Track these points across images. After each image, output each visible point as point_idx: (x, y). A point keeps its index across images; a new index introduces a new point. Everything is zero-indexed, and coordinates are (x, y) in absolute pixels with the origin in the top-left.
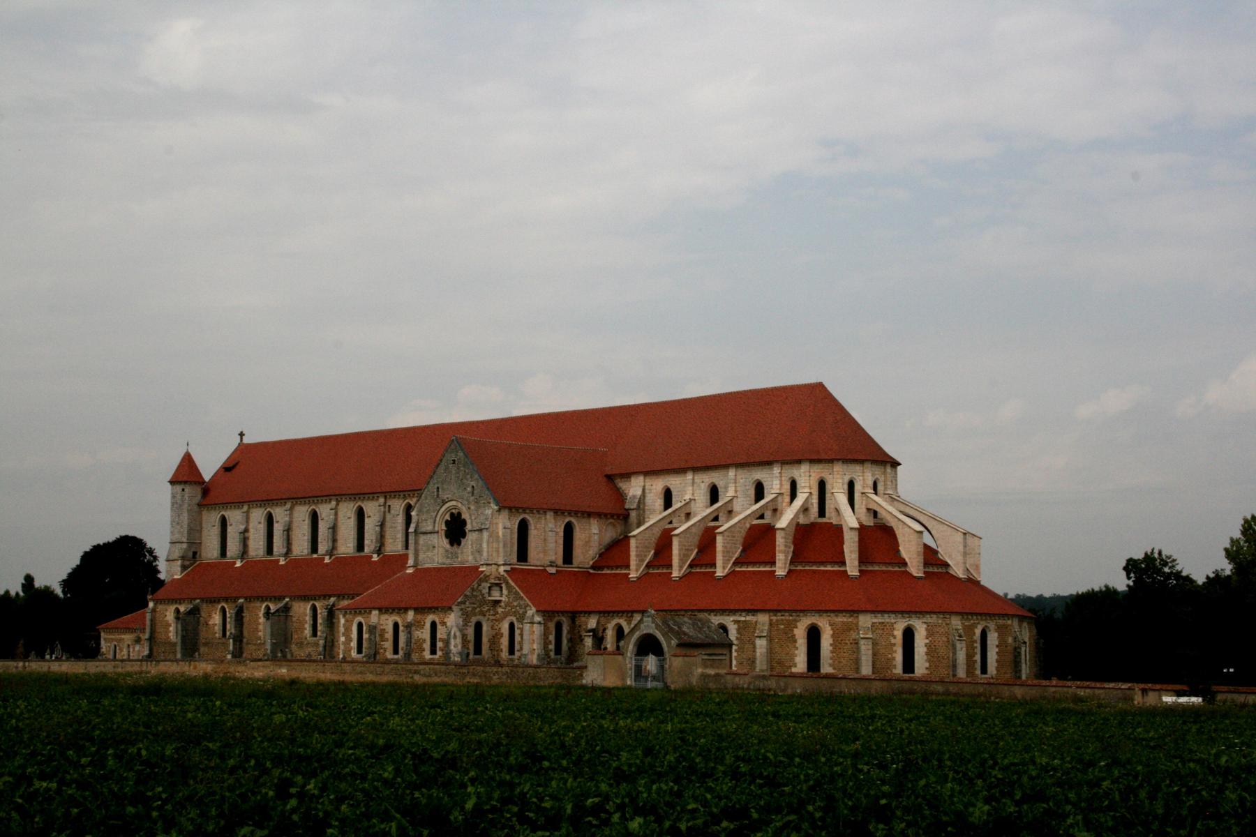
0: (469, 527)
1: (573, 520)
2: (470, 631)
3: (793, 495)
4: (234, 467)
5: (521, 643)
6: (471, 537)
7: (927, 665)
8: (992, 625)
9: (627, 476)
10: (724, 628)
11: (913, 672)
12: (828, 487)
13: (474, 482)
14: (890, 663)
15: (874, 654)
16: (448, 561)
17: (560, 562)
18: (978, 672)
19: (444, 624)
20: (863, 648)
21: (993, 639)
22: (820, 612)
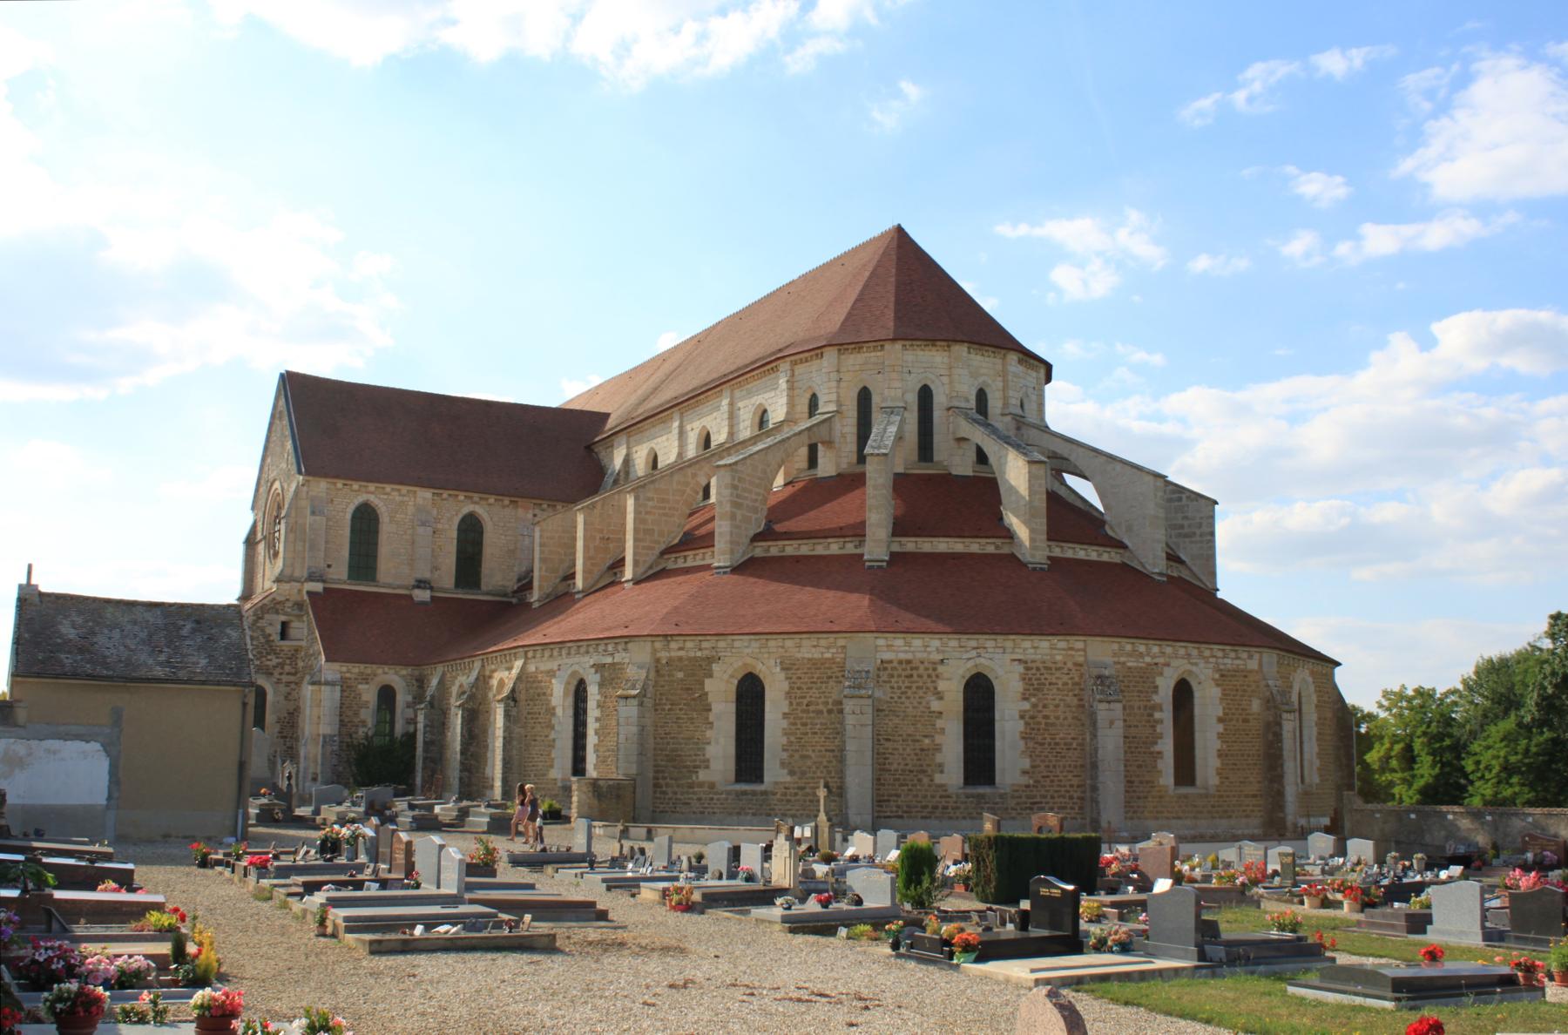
1: (480, 510)
7: (1026, 763)
11: (990, 779)
14: (925, 759)
15: (877, 739)
17: (446, 577)
18: (1167, 777)
20: (850, 720)
21: (1208, 703)
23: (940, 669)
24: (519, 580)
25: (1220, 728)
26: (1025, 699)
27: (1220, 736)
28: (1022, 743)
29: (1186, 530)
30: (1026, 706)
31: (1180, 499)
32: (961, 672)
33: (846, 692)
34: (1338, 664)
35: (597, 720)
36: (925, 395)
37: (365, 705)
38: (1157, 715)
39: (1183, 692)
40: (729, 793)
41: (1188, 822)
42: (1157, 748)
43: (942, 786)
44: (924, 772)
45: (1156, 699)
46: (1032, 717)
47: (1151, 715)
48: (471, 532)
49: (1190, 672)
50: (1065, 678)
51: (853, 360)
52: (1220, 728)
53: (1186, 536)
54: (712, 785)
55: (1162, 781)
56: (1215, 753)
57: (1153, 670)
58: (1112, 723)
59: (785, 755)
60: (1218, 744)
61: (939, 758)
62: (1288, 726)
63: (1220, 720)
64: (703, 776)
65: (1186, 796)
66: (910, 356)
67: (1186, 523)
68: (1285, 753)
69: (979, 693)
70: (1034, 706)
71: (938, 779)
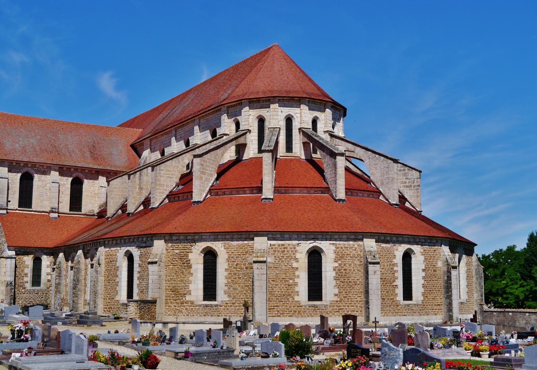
7: (336, 291)
8: (417, 249)
11: (320, 299)
12: (267, 125)
17: (65, 207)
20: (256, 272)
21: (418, 263)
22: (217, 236)
23: (297, 248)
24: (100, 207)
25: (424, 274)
26: (336, 261)
27: (424, 278)
28: (335, 281)
29: (407, 184)
30: (336, 265)
31: (404, 170)
32: (307, 249)
33: (254, 259)
34: (476, 245)
35: (139, 272)
37: (27, 267)
38: (395, 269)
40: (200, 306)
41: (409, 317)
42: (395, 284)
43: (298, 301)
44: (290, 295)
45: (395, 261)
46: (339, 270)
47: (392, 269)
49: (410, 249)
50: (354, 252)
52: (424, 274)
53: (407, 187)
54: (192, 303)
55: (398, 299)
56: (421, 286)
58: (375, 272)
59: (226, 288)
60: (423, 282)
61: (297, 289)
62: (454, 273)
63: (424, 270)
64: (188, 298)
65: (408, 305)
67: (407, 181)
68: (453, 285)
70: (340, 265)
71: (296, 298)
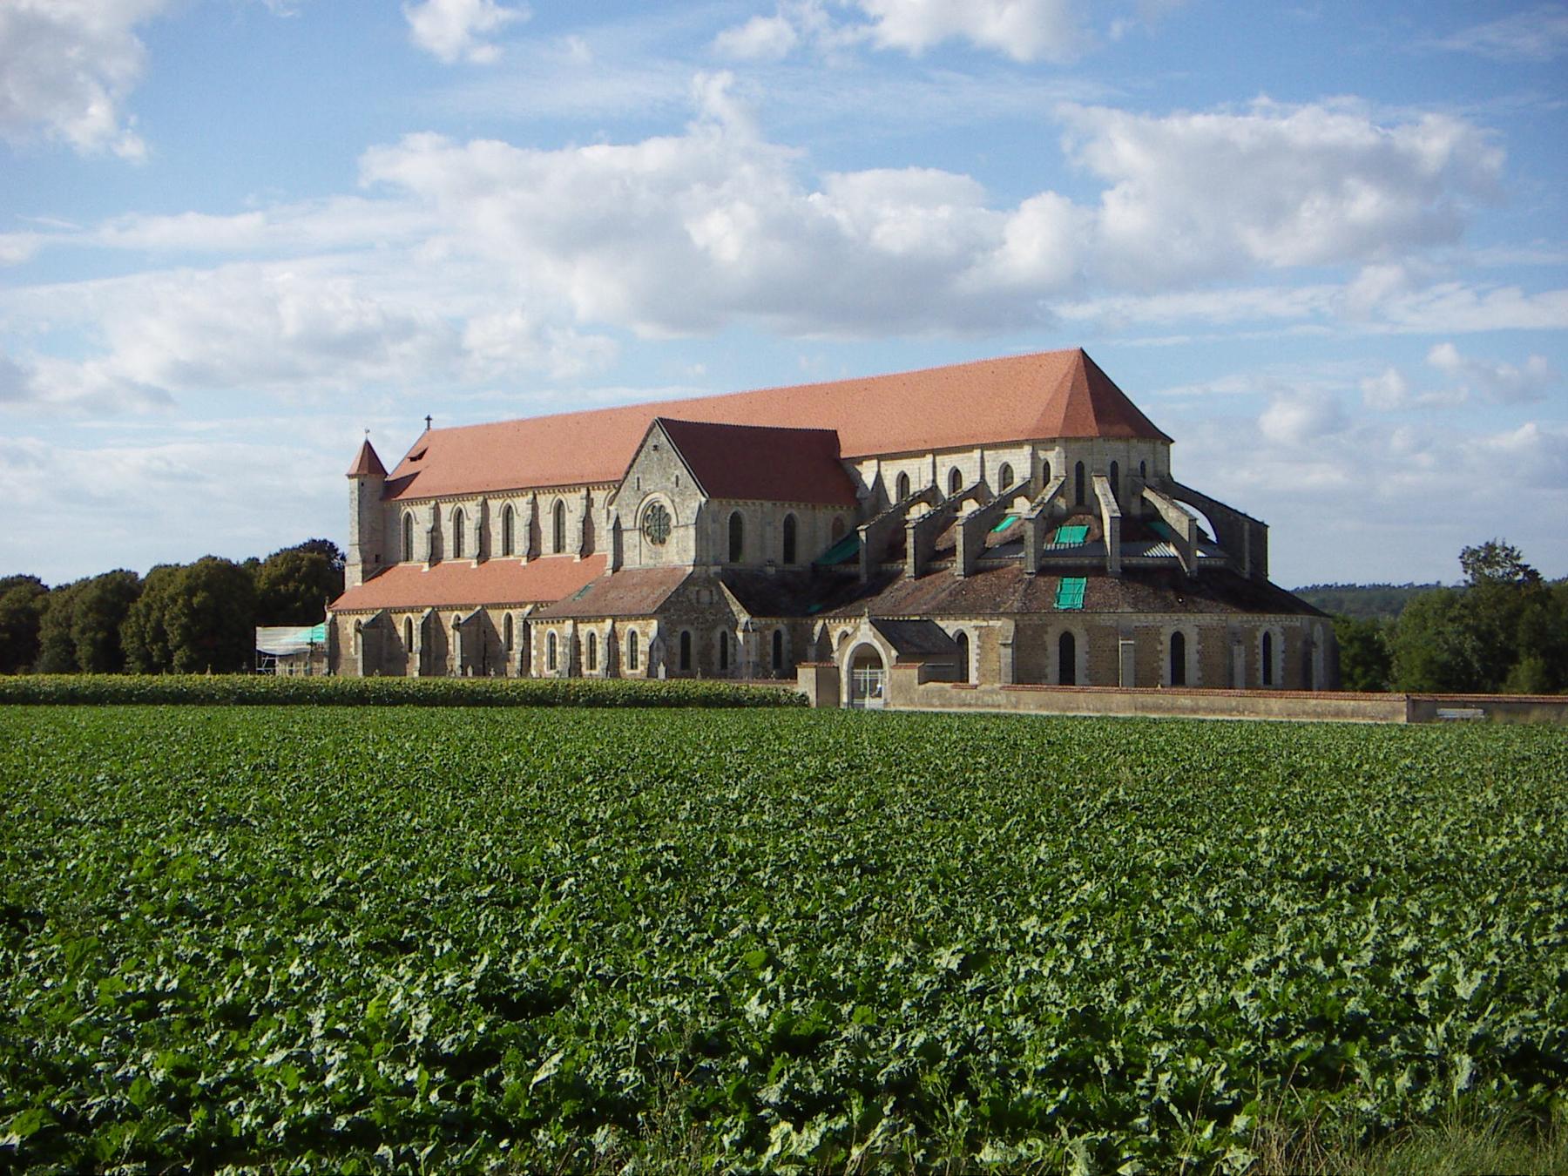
0: (674, 522)
1: (795, 512)
2: (676, 642)
3: (1047, 481)
4: (421, 456)
5: (734, 655)
6: (674, 533)
9: (860, 460)
10: (962, 638)
13: (680, 470)
15: (1137, 663)
16: (652, 562)
17: (779, 556)
19: (645, 634)
36: (1114, 465)
39: (1267, 638)
48: (790, 524)
51: (1074, 446)
57: (1256, 628)
66: (1107, 445)
69: (1178, 640)
